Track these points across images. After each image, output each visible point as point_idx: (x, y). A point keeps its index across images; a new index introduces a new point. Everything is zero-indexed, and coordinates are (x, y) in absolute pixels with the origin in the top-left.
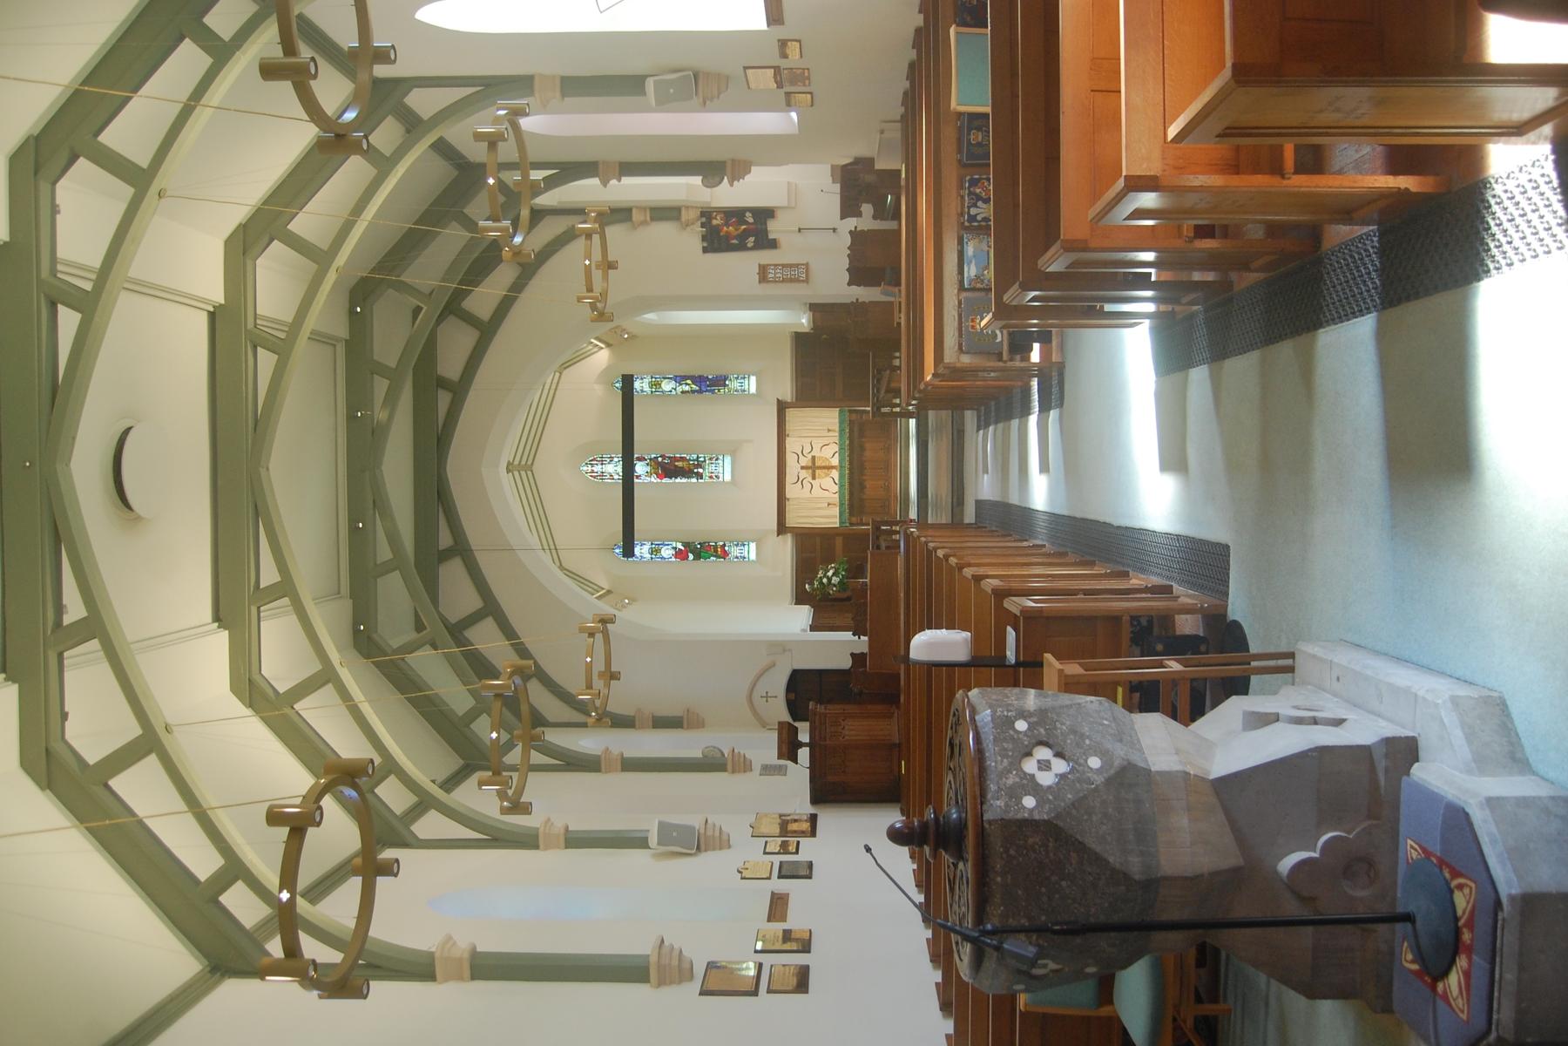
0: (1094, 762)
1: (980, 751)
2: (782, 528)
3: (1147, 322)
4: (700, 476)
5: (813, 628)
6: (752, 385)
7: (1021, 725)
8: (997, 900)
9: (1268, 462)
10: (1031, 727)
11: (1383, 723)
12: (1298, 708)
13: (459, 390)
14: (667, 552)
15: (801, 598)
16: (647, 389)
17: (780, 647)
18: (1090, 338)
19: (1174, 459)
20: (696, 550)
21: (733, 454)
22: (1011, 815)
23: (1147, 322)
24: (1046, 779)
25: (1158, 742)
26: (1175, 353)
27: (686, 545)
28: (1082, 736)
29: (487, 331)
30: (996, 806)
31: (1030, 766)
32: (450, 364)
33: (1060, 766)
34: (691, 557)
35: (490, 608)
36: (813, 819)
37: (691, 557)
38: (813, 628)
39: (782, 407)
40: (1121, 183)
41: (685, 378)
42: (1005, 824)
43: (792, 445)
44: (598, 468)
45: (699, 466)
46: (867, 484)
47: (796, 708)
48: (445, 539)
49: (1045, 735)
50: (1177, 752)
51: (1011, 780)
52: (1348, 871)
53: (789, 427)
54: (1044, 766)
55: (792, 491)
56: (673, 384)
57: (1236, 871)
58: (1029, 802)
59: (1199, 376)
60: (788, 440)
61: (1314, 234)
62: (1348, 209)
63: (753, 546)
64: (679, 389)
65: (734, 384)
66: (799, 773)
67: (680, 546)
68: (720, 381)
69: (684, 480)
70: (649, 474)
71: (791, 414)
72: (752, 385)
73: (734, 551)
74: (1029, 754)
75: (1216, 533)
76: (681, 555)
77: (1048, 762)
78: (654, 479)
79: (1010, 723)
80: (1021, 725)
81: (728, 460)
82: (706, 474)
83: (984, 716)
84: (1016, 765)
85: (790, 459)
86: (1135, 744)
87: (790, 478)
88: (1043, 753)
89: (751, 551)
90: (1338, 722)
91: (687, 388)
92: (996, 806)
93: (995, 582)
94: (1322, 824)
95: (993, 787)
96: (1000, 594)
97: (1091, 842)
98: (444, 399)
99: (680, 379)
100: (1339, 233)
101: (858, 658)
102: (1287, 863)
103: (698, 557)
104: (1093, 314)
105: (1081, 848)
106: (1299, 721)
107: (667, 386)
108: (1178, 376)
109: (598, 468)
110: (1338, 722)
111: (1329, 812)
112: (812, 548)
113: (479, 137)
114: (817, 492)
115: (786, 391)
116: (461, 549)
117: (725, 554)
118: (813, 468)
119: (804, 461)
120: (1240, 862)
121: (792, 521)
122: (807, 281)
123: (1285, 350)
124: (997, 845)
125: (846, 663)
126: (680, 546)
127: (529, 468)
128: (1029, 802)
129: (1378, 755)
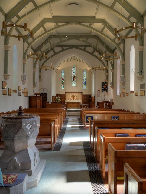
0: (29, 133)
1: (31, 118)
3: (89, 140)
5: (52, 96)
6: (85, 89)
7: (34, 123)
8: (11, 120)
9: (70, 156)
10: (34, 125)
11: (34, 171)
12: (37, 160)
13: (84, 50)
14: (63, 77)
15: (57, 95)
17: (50, 92)
18: (88, 132)
19: (72, 144)
20: (63, 81)
21: (76, 86)
22: (22, 122)
23: (89, 140)
24: (27, 127)
25: (32, 141)
26: (85, 144)
27: (64, 80)
28: (33, 131)
29: (92, 54)
30: (23, 120)
31: (29, 125)
32: (88, 49)
33: (29, 128)
35: (55, 54)
36: (27, 96)
38: (52, 96)
39: (82, 93)
40: (104, 137)
42: (21, 121)
43: (77, 94)
46: (71, 104)
47: (42, 94)
48: (65, 48)
49: (33, 127)
50: (31, 144)
51: (27, 122)
52: (14, 166)
53: (79, 94)
54: (29, 126)
55: (71, 94)
57: (15, 151)
58: (24, 124)
59: (82, 147)
60: (77, 94)
61: (98, 162)
62: (101, 166)
63: (64, 89)
66: (33, 94)
71: (81, 94)
73: (63, 86)
74: (31, 124)
75: (62, 149)
76: (62, 79)
77: (29, 127)
78: (73, 76)
79: (35, 122)
80: (34, 123)
81: (75, 85)
83: (36, 119)
84: (29, 123)
85: (75, 94)
86: (32, 138)
87: (72, 94)
88: (31, 126)
90: (34, 165)
92: (23, 120)
93: (56, 121)
94: (21, 163)
95: (26, 120)
96: (54, 121)
97: (19, 132)
98: (83, 48)
99: (86, 79)
100: (99, 165)
101: (48, 102)
102: (16, 158)
103: (62, 81)
104: (91, 134)
105: (18, 131)
106: (35, 160)
107: (85, 78)
108: (82, 144)
110: (34, 165)
111: (23, 164)
112: (63, 97)
113: (116, 53)
114: (70, 97)
115: (84, 93)
116: (63, 50)
118: (74, 97)
119: (75, 95)
120: (16, 152)
121: (66, 94)
122: (98, 96)
123: (84, 158)
124: (18, 120)
125: (48, 101)
127: (74, 59)
128: (24, 124)
129: (30, 170)
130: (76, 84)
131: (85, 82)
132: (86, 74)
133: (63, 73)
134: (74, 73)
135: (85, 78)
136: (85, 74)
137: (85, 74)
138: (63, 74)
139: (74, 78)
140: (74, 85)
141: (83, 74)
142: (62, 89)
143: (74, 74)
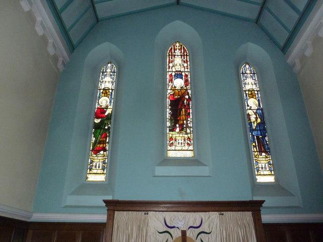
2: (113, 206)
4: (173, 129)
6: (266, 178)
14: (104, 101)
16: (248, 87)
27: (109, 117)
34: (97, 121)
37: (97, 121)
41: (262, 116)
43: (212, 219)
44: (178, 52)
45: (182, 129)
55: (155, 220)
56: (255, 107)
60: (214, 215)
64: (250, 112)
65: (263, 161)
67: (108, 111)
68: (263, 148)
69: (168, 116)
70: (174, 88)
71: (248, 216)
72: (266, 178)
73: (98, 160)
81: (190, 154)
82: (175, 134)
89: (97, 177)
91: (253, 118)
99: (261, 113)
103: (97, 127)
107: (252, 103)
109: (178, 52)
117: (96, 151)
126: (108, 111)
130: (196, 142)
131: (262, 126)
132: (261, 81)
133: (108, 79)
134: (179, 75)
135: (252, 103)
136: (250, 84)
137: (250, 84)
138: (107, 82)
139: (178, 104)
140: (180, 148)
141: (239, 84)
142: (91, 178)
143: (179, 83)
